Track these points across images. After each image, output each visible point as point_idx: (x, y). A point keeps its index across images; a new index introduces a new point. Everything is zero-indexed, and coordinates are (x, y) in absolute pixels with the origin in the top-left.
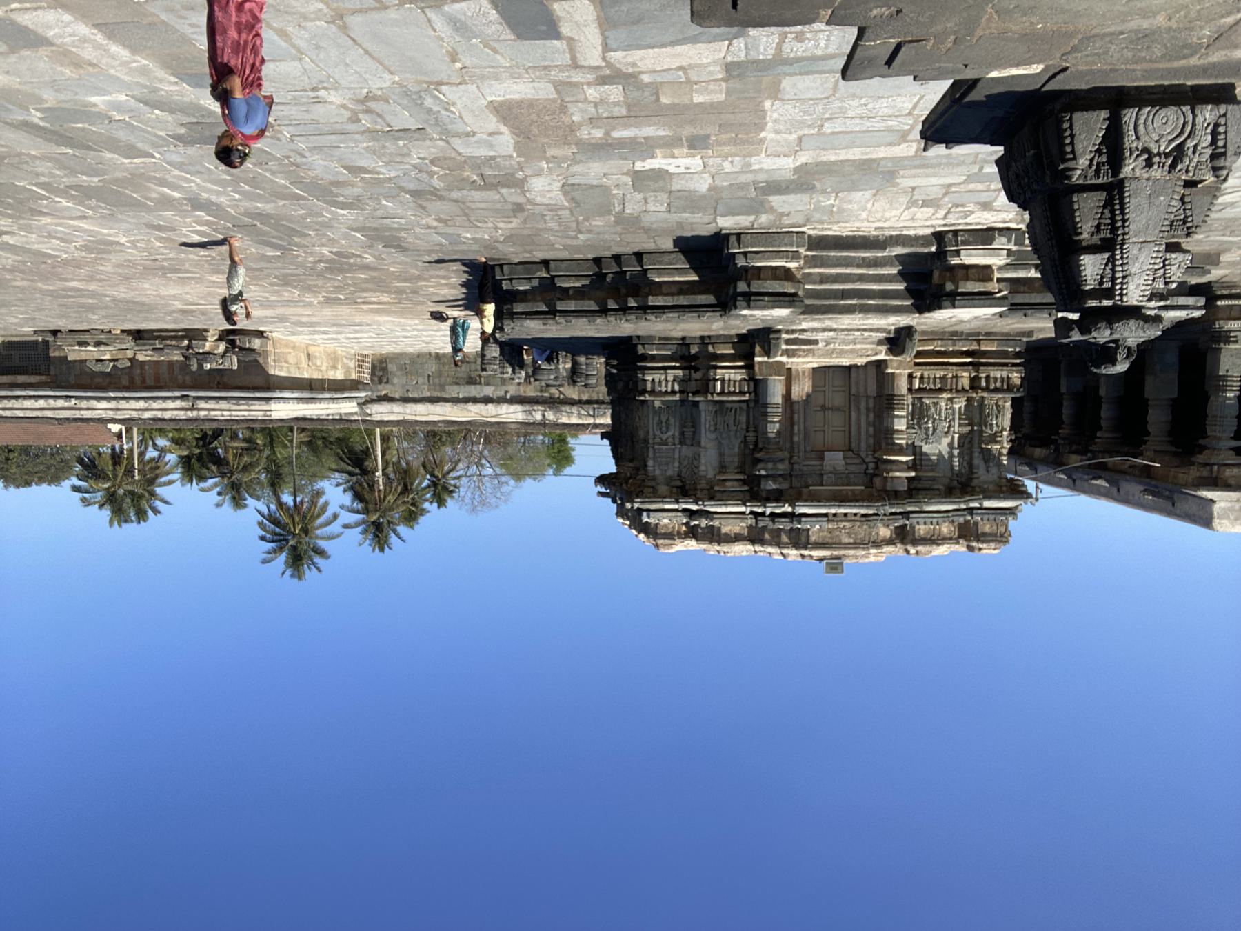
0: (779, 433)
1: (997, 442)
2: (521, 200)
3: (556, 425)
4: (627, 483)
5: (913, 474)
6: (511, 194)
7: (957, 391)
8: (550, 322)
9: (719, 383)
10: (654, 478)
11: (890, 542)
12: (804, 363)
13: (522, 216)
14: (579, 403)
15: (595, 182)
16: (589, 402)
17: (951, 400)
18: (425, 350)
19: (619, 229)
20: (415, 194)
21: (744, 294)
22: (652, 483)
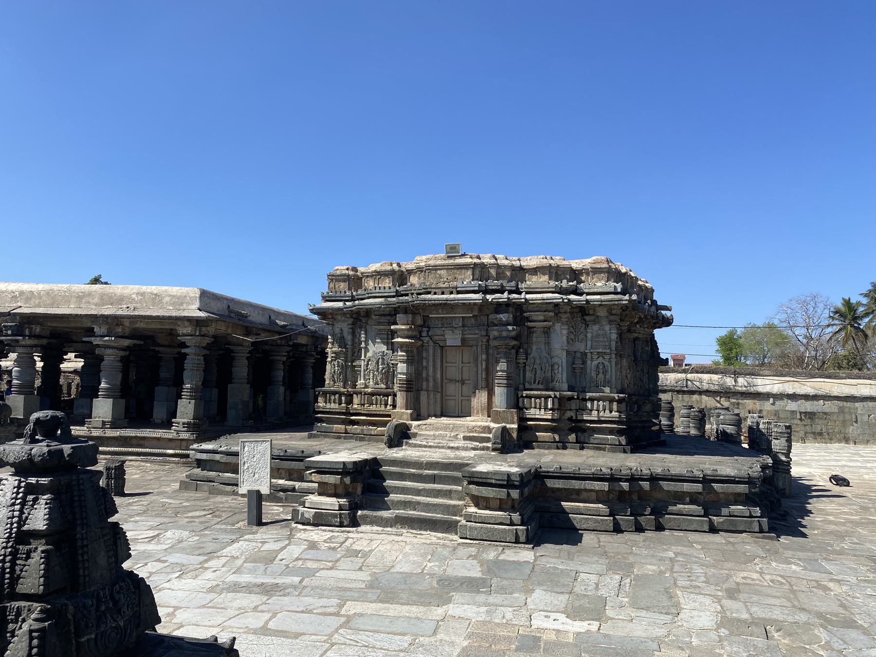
0: (498, 362)
1: (335, 353)
2: (727, 603)
3: (724, 372)
4: (640, 318)
5: (392, 327)
6: (737, 611)
7: (361, 393)
8: (709, 472)
9: (550, 406)
10: (610, 322)
11: (410, 272)
12: (477, 421)
13: (730, 584)
14: (701, 392)
15: (644, 613)
16: (692, 392)
17: (366, 387)
18: (860, 447)
19: (632, 559)
20: (850, 624)
21: (514, 487)
22: (612, 318)
